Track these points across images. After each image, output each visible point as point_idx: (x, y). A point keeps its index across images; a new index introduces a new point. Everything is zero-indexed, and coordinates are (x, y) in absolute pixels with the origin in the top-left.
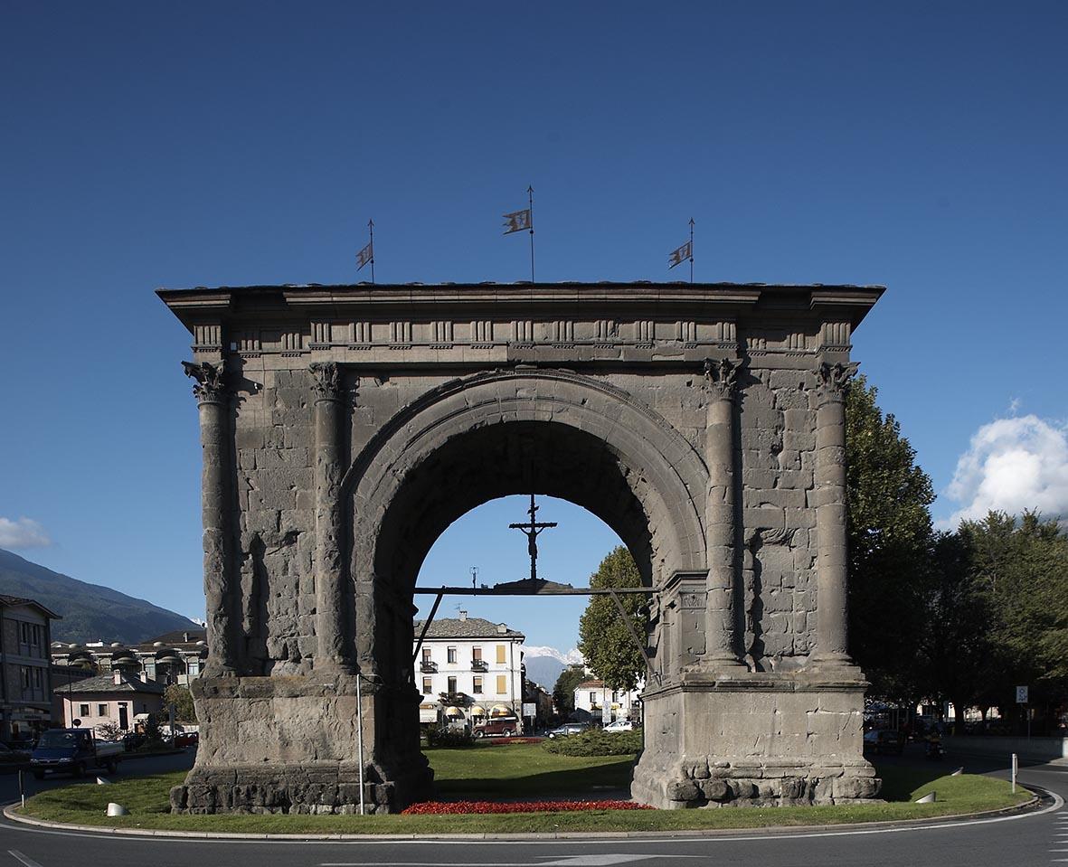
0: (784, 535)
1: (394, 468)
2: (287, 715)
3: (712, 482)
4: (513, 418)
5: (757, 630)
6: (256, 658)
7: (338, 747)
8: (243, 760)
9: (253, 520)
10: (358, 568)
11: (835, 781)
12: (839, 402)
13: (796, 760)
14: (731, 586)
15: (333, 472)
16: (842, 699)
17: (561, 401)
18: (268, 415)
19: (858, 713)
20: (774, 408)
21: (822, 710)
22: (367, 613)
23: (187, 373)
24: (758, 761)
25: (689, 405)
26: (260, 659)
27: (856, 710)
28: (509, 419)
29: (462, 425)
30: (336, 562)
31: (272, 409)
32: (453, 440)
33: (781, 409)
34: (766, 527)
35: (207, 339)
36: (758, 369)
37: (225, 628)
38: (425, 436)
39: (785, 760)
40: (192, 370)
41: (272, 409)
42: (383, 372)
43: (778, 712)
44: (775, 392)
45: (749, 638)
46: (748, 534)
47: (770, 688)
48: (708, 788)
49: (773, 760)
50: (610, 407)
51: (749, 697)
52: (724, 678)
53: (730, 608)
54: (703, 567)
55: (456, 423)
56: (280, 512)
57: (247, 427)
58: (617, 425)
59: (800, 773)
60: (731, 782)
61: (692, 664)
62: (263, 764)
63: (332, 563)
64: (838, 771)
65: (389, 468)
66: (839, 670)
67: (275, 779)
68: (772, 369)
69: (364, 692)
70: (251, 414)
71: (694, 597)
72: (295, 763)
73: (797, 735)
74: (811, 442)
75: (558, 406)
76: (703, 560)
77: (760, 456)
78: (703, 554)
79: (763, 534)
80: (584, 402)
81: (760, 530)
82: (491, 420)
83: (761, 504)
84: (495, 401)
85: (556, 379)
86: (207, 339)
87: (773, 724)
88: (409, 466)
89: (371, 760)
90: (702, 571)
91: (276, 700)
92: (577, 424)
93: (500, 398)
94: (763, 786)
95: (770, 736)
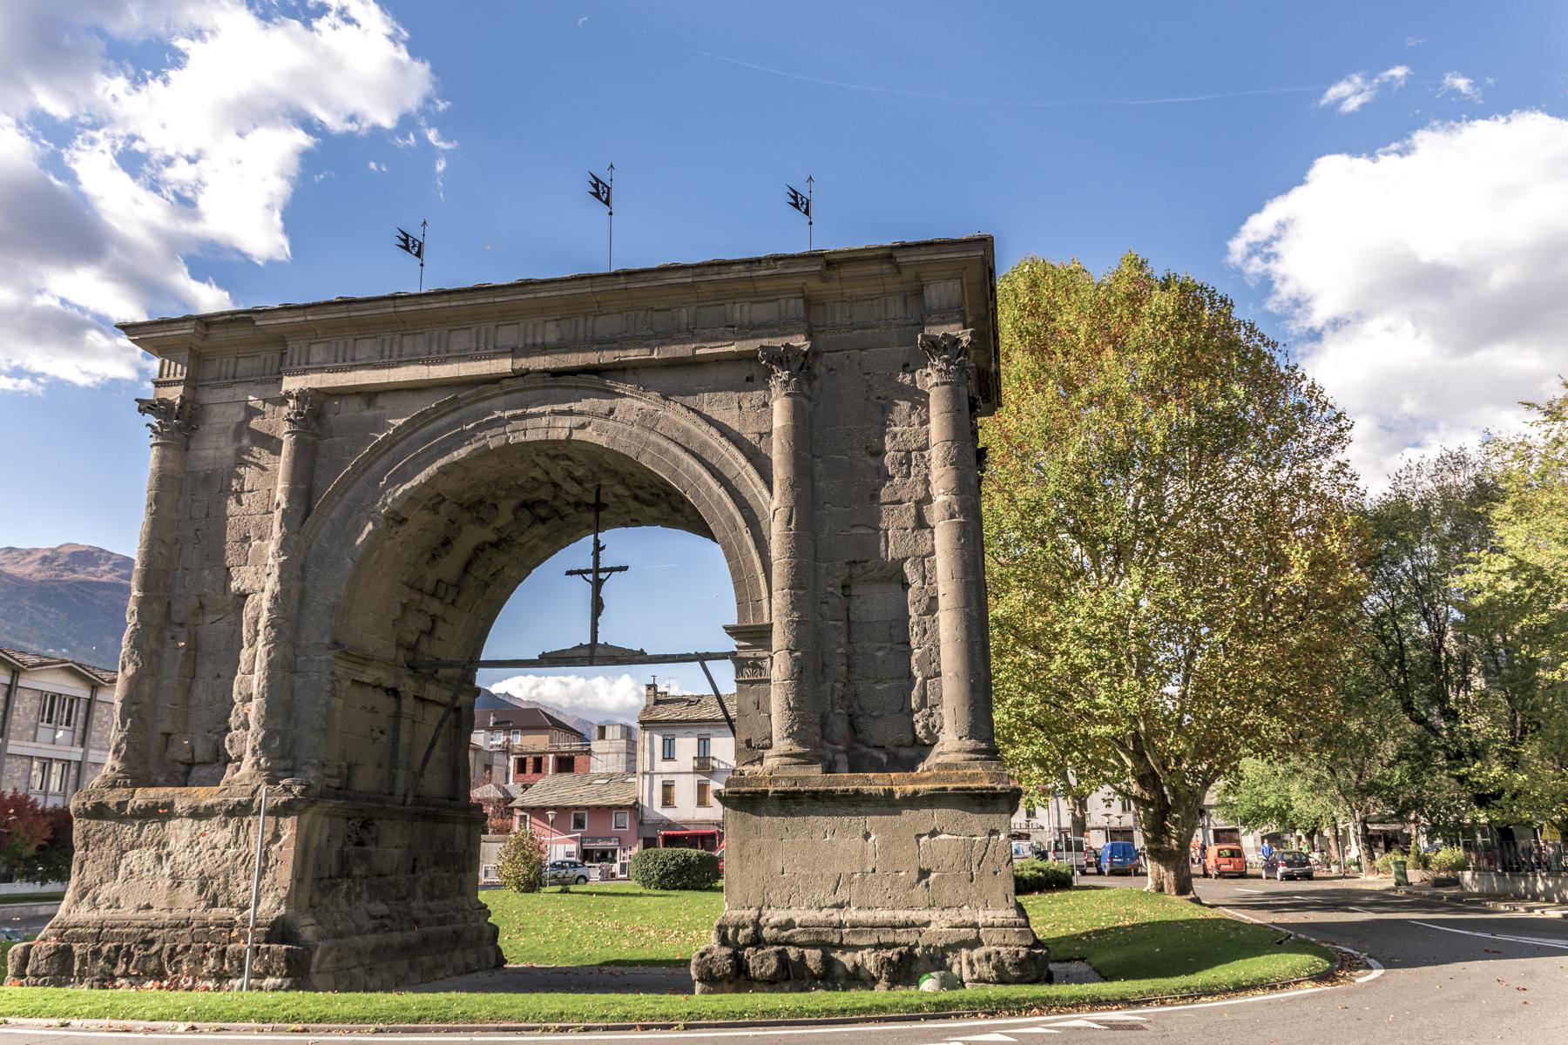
3: (775, 504)
6: (175, 761)
7: (243, 888)
8: (118, 907)
11: (964, 952)
13: (902, 915)
23: (140, 410)
26: (183, 763)
28: (516, 440)
31: (236, 445)
34: (858, 558)
35: (172, 371)
39: (883, 915)
40: (146, 407)
41: (236, 445)
44: (868, 377)
48: (762, 962)
49: (863, 916)
52: (783, 786)
54: (766, 621)
57: (206, 468)
58: (653, 437)
59: (904, 937)
60: (793, 953)
61: (752, 763)
64: (971, 934)
67: (150, 935)
69: (278, 812)
70: (211, 453)
73: (903, 874)
74: (921, 438)
75: (576, 420)
76: (766, 611)
78: (765, 603)
79: (858, 570)
81: (852, 564)
85: (577, 387)
86: (172, 371)
92: (603, 441)
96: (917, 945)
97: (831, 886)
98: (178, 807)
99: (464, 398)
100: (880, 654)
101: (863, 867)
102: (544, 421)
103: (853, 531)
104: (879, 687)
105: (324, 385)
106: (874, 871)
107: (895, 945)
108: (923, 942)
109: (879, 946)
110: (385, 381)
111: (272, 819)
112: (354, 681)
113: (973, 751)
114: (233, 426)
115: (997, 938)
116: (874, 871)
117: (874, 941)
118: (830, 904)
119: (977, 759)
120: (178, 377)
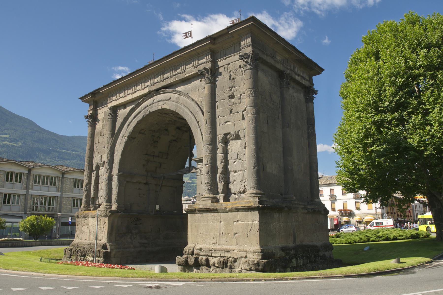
0: (235, 135)
1: (124, 136)
2: (91, 224)
4: (153, 110)
5: (227, 182)
9: (96, 160)
10: (114, 172)
12: (248, 69)
13: (229, 247)
14: (209, 163)
15: (109, 141)
16: (249, 214)
17: (163, 101)
18: (102, 126)
19: (256, 222)
20: (230, 80)
21: (240, 221)
22: (116, 187)
24: (213, 247)
25: (200, 89)
27: (254, 220)
29: (140, 117)
30: (108, 170)
32: (139, 123)
33: (233, 79)
36: (223, 66)
37: (86, 195)
38: (132, 123)
41: (103, 124)
42: (124, 105)
43: (222, 223)
44: (230, 73)
45: (221, 186)
46: (219, 137)
47: (216, 211)
50: (177, 98)
51: (210, 215)
52: (201, 206)
53: (208, 173)
55: (139, 117)
56: (102, 156)
59: (227, 255)
62: (85, 241)
63: (106, 171)
64: (244, 254)
65: (123, 136)
66: (248, 199)
68: (229, 64)
71: (200, 170)
72: (91, 241)
73: (229, 234)
75: (163, 102)
77: (225, 102)
79: (228, 137)
80: (170, 98)
82: (147, 113)
83: (226, 122)
84: (147, 106)
87: (220, 229)
88: (128, 134)
89: (106, 242)
90: (201, 158)
91: (90, 219)
93: (149, 104)
94: (212, 261)
95: (218, 235)
96: (230, 257)
97: (212, 238)
98: (90, 216)
99: (141, 102)
100: (235, 163)
101: (220, 232)
102: (156, 104)
103: (226, 124)
104: (236, 174)
105: (115, 105)
106: (223, 233)
107: (224, 257)
108: (232, 256)
109: (221, 257)
110: (125, 101)
111: (104, 218)
112: (127, 182)
113: (256, 194)
114: (102, 119)
115: (251, 256)
116: (223, 233)
117: (220, 255)
118: (212, 243)
119: (255, 196)
120: (91, 109)
